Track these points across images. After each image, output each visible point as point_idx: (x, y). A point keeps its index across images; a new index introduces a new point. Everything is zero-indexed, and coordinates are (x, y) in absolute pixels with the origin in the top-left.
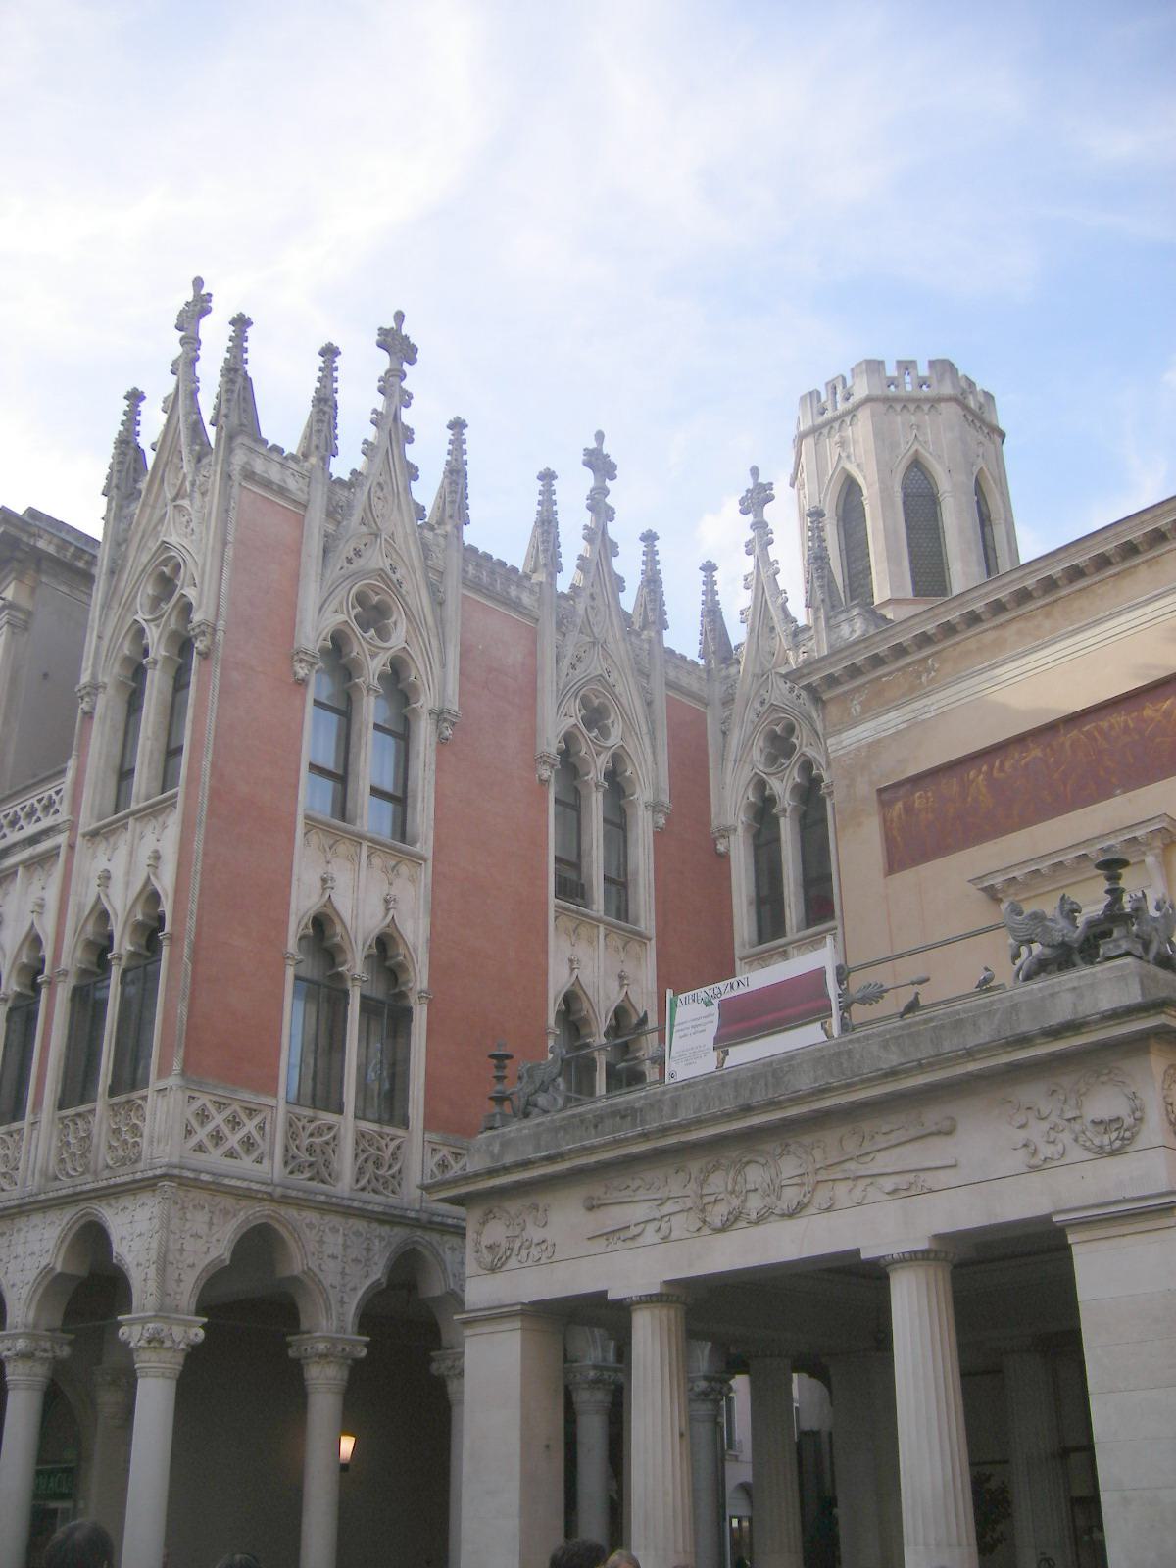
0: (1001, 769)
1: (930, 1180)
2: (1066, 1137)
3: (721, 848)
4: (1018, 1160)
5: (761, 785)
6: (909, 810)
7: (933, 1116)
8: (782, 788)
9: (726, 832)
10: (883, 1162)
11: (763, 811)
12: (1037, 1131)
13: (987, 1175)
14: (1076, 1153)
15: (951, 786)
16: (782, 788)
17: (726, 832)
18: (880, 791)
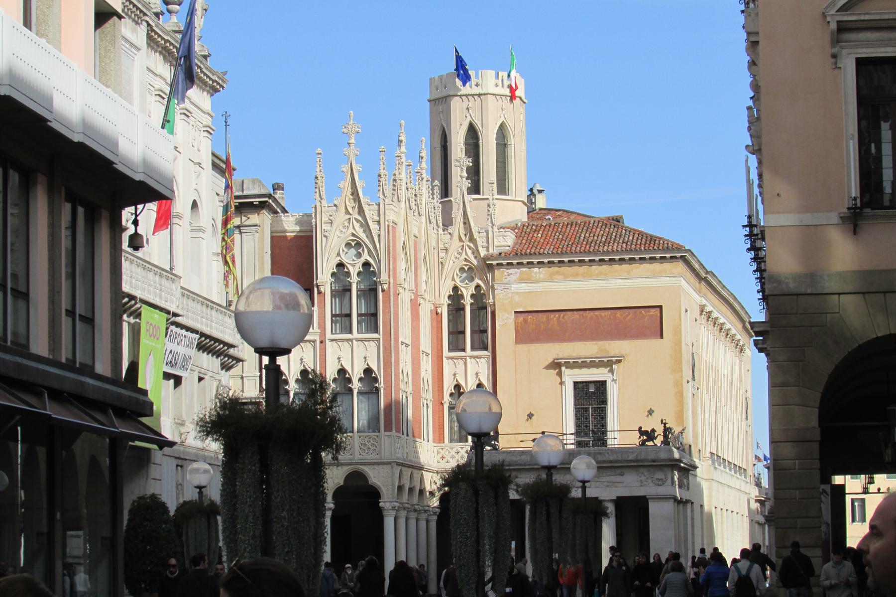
0: (563, 318)
1: (617, 485)
2: (650, 481)
3: (439, 311)
4: (638, 484)
5: (455, 288)
6: (525, 321)
7: (618, 471)
8: (467, 292)
9: (440, 306)
10: (604, 479)
11: (456, 297)
12: (643, 478)
13: (631, 485)
14: (651, 484)
15: (543, 317)
16: (467, 292)
17: (440, 306)
18: (515, 312)
